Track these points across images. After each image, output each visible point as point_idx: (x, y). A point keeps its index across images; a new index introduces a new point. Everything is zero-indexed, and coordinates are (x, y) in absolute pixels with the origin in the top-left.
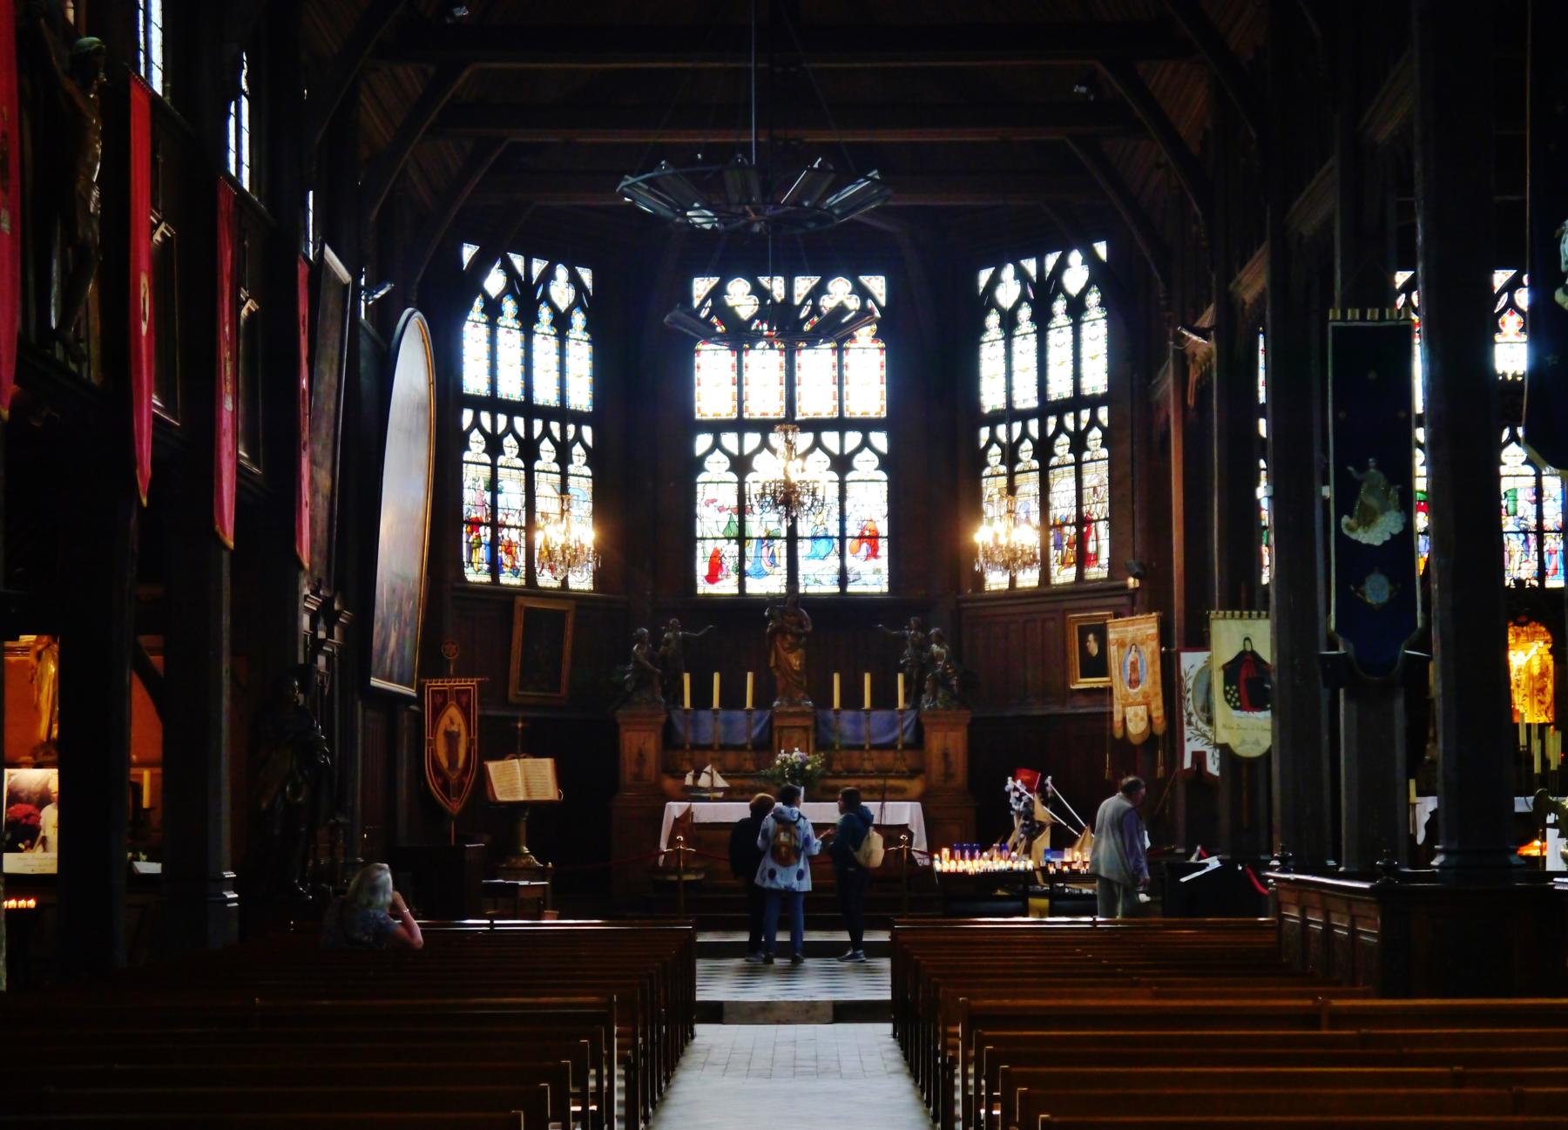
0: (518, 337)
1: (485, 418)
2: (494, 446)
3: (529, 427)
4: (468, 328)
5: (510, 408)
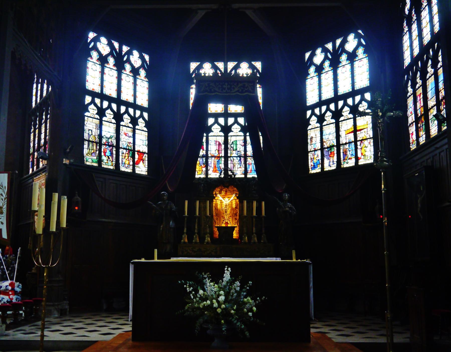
0: (115, 73)
1: (98, 101)
3: (119, 109)
4: (90, 65)
5: (110, 99)
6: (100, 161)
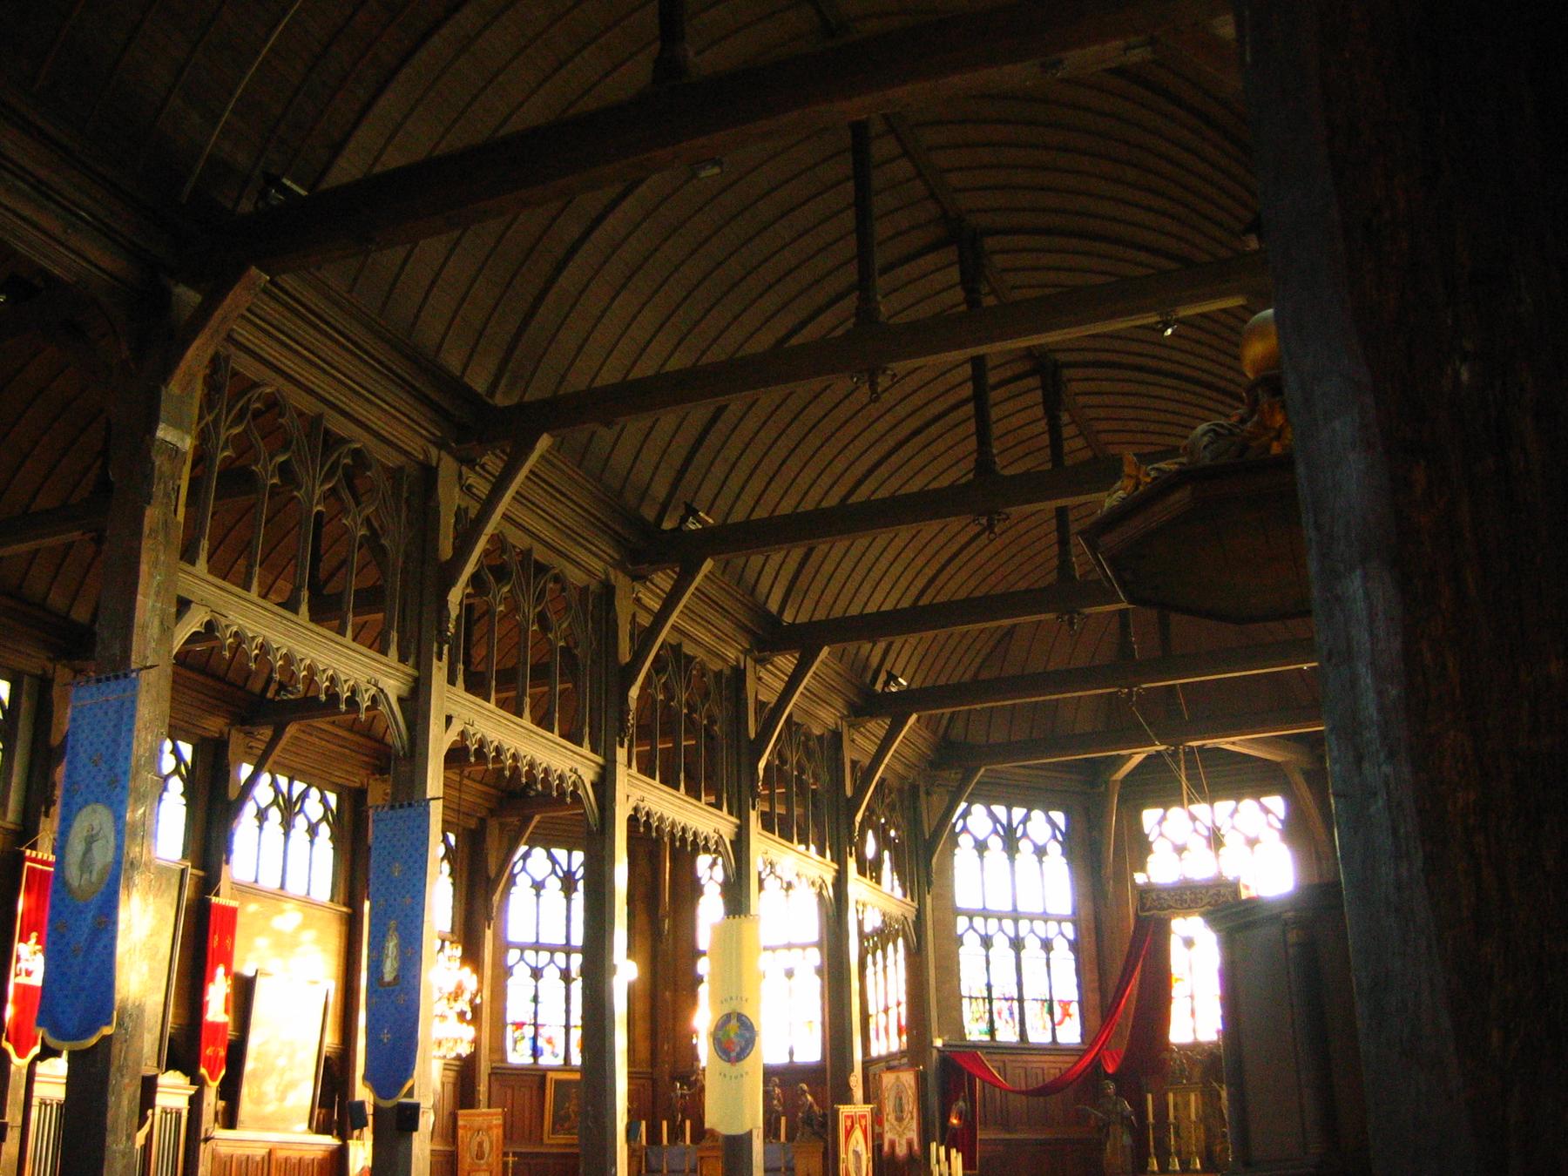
2: (987, 942)
6: (992, 1031)
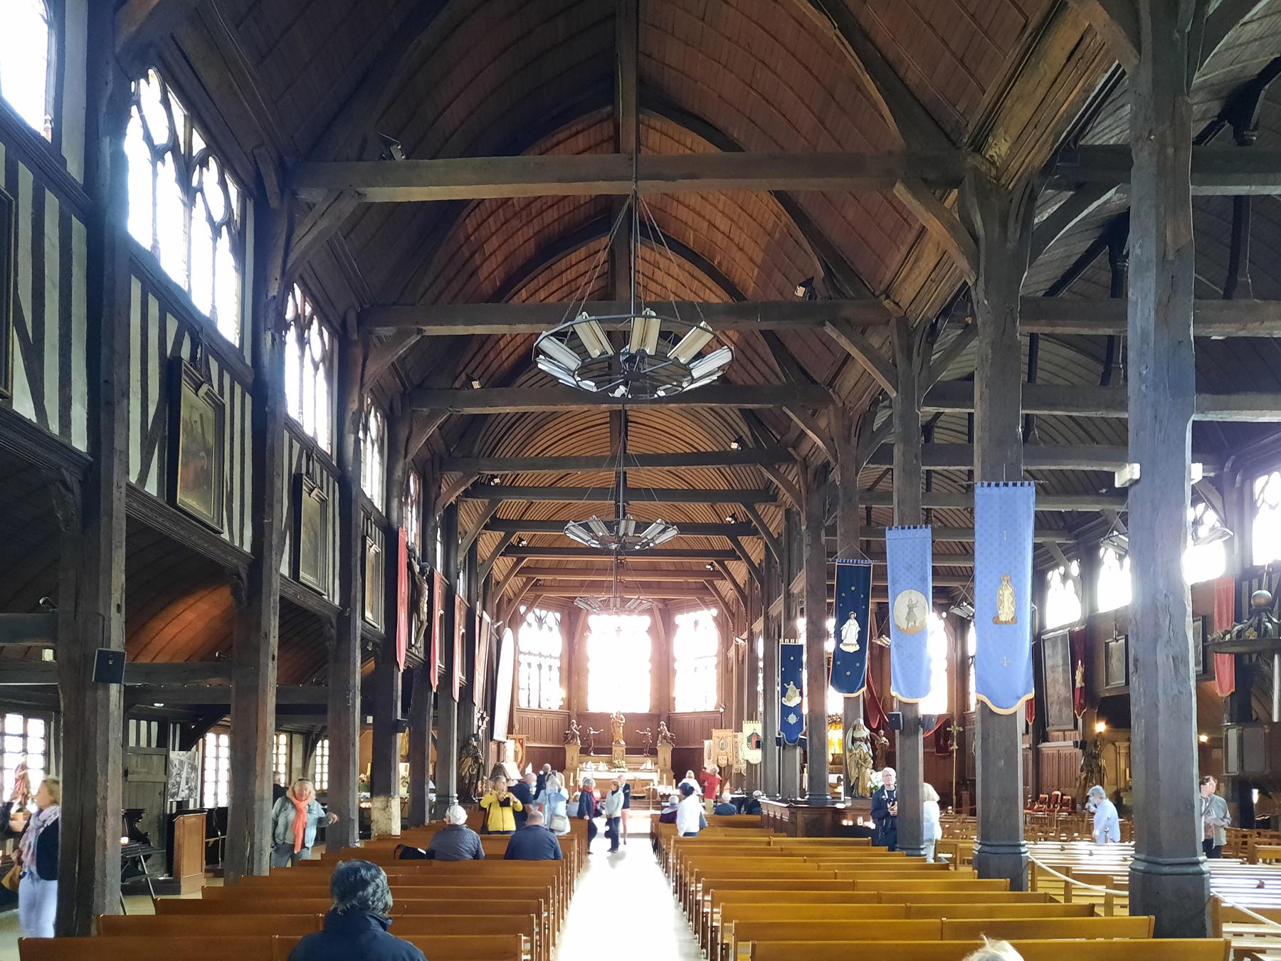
2: (529, 665)
